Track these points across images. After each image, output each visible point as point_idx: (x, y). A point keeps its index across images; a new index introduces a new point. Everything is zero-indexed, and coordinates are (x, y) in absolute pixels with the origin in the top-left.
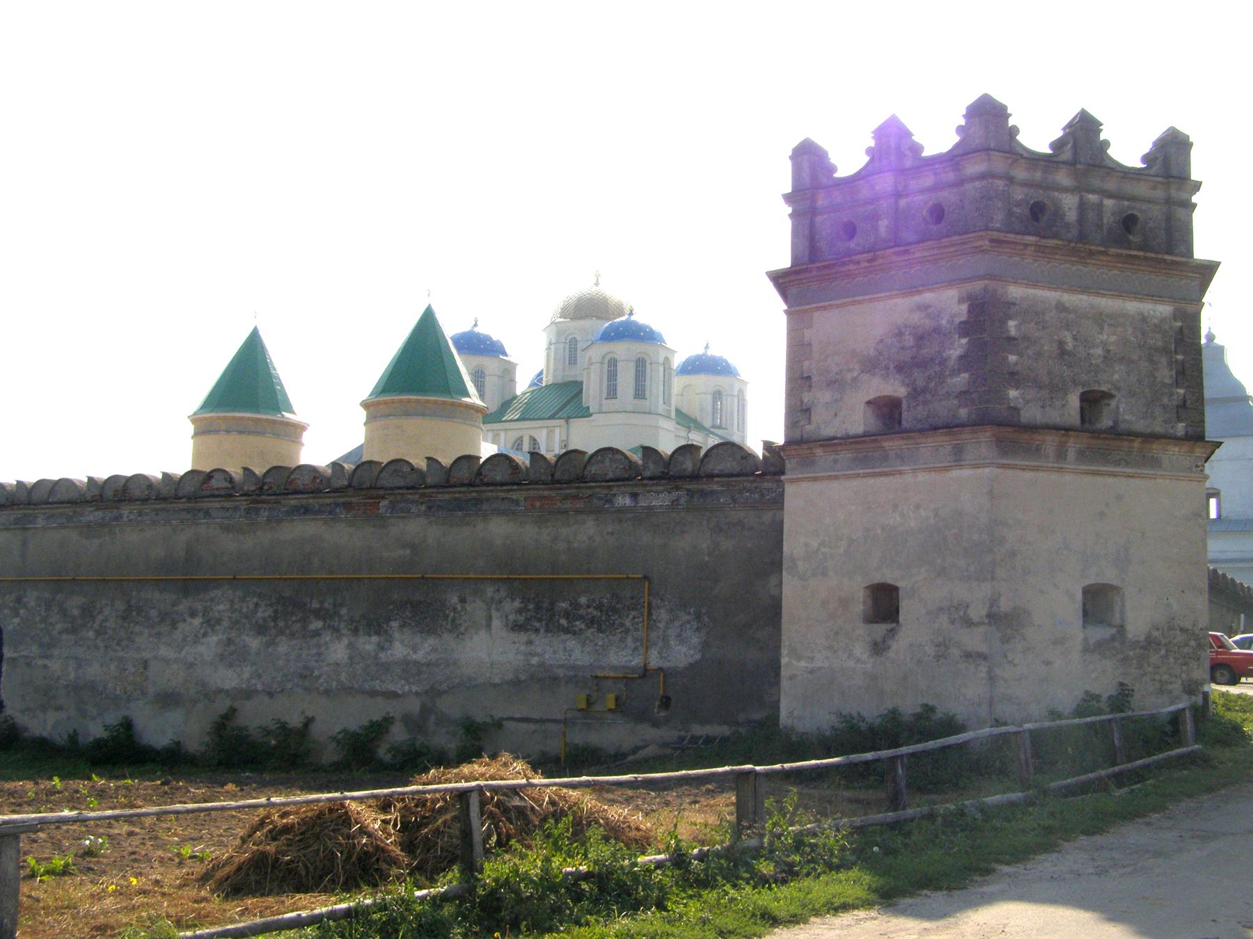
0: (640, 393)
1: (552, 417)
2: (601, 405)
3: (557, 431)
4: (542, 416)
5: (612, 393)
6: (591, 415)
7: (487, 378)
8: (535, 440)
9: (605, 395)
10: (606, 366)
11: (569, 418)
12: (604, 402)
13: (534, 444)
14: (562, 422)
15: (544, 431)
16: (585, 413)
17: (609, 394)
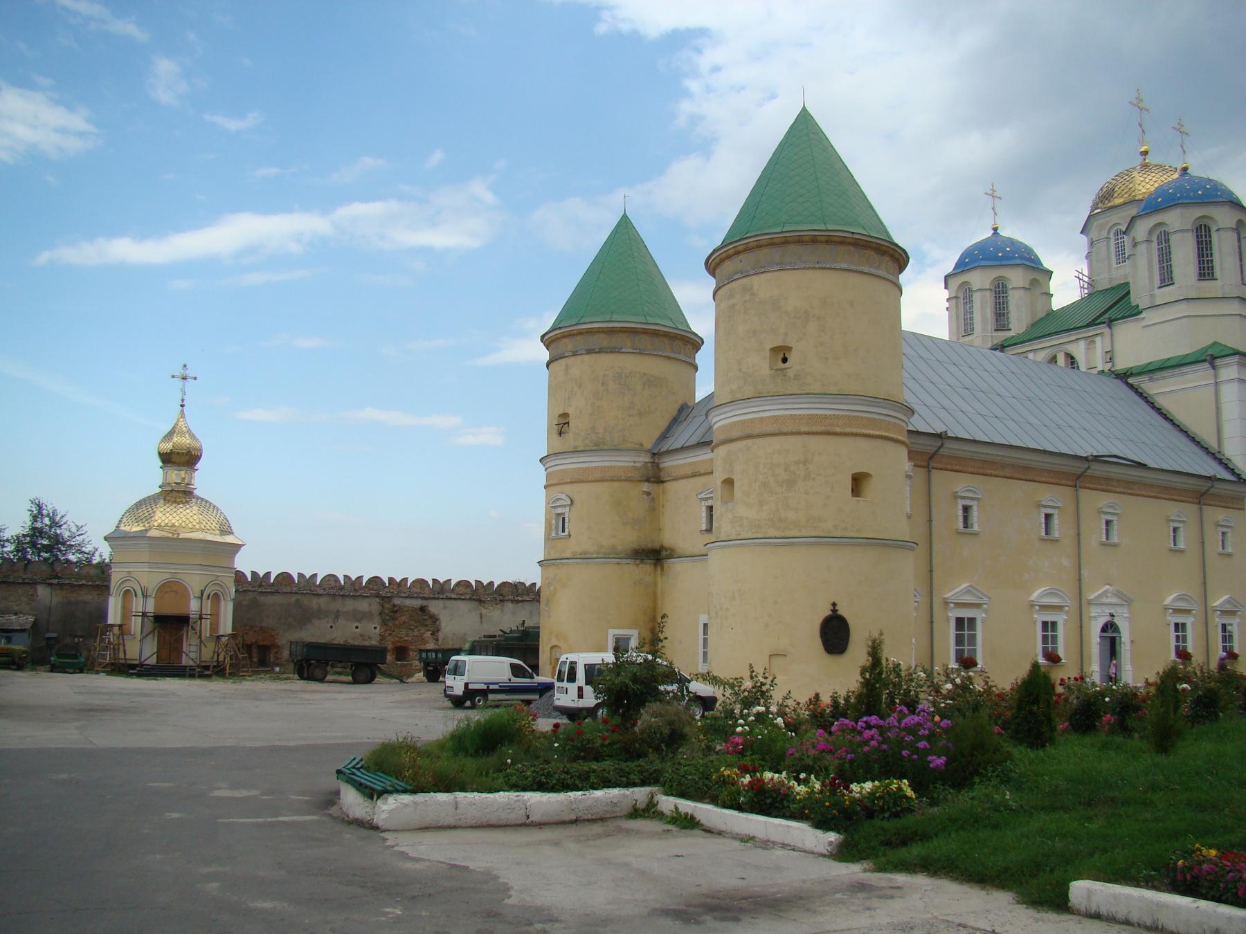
0: (1206, 271)
1: (1092, 324)
2: (1153, 296)
3: (1098, 340)
4: (1078, 326)
5: (1167, 279)
6: (1142, 312)
7: (1010, 293)
8: (1072, 358)
9: (1157, 282)
10: (1155, 246)
11: (1110, 323)
12: (1157, 292)
13: (1072, 363)
14: (1105, 330)
15: (1082, 344)
16: (1135, 312)
17: (1162, 280)
